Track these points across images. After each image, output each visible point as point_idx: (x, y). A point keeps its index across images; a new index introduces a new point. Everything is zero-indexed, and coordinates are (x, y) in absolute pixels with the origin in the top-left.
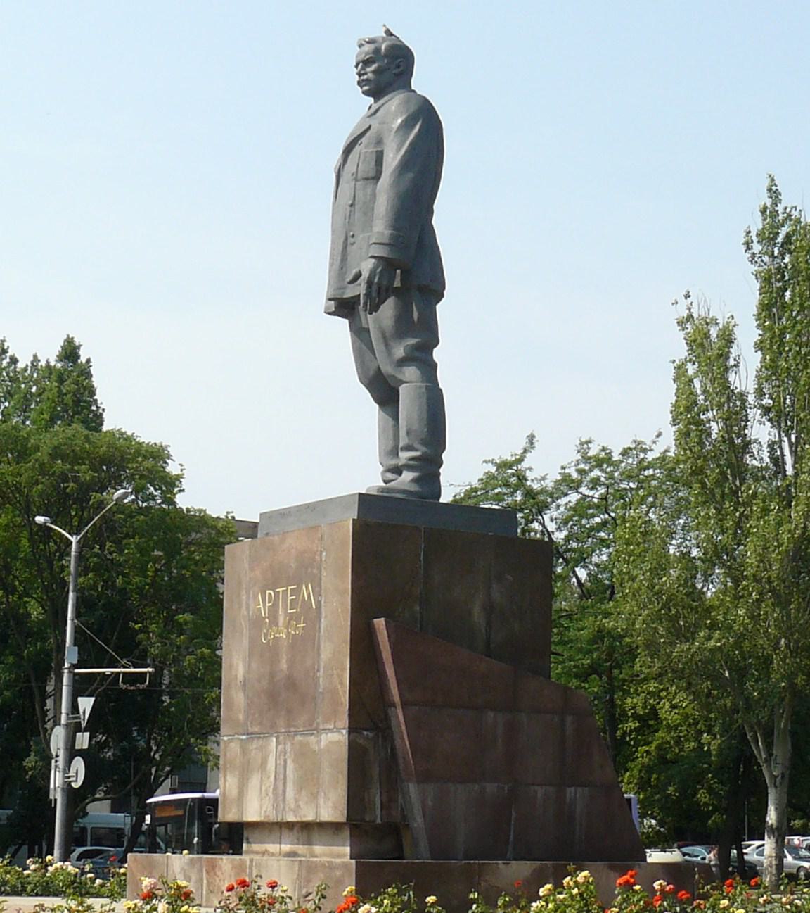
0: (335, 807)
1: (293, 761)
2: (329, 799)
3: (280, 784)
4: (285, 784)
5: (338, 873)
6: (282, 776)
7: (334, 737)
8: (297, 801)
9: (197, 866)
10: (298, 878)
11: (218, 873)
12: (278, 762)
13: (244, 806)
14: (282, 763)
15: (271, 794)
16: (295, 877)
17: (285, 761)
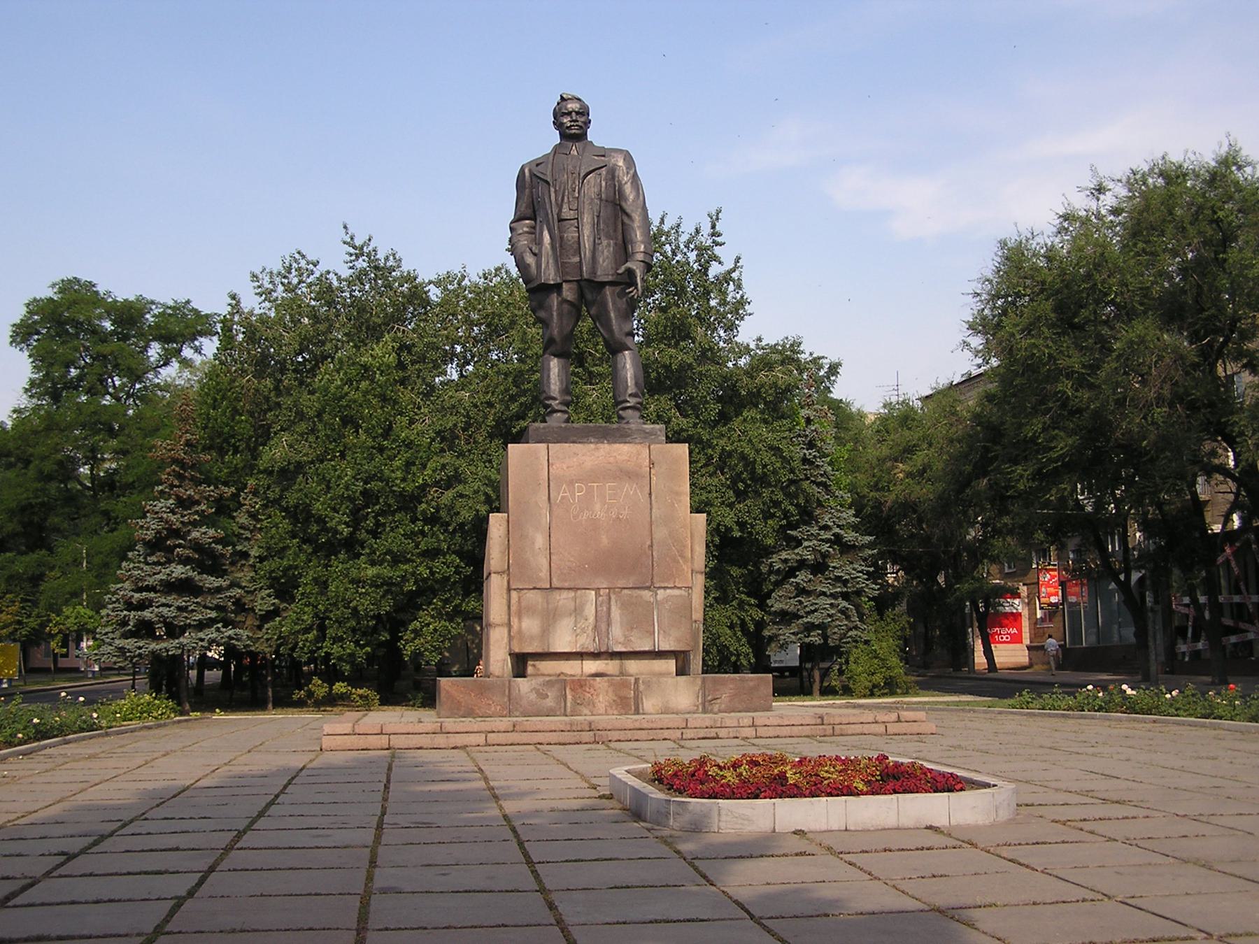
0: (678, 641)
1: (620, 608)
2: (670, 635)
3: (603, 626)
4: (609, 624)
5: (751, 684)
6: (605, 619)
7: (676, 592)
8: (626, 637)
9: (557, 686)
10: (701, 689)
11: (588, 690)
12: (599, 609)
13: (551, 641)
14: (605, 609)
15: (590, 631)
16: (697, 688)
17: (609, 609)
